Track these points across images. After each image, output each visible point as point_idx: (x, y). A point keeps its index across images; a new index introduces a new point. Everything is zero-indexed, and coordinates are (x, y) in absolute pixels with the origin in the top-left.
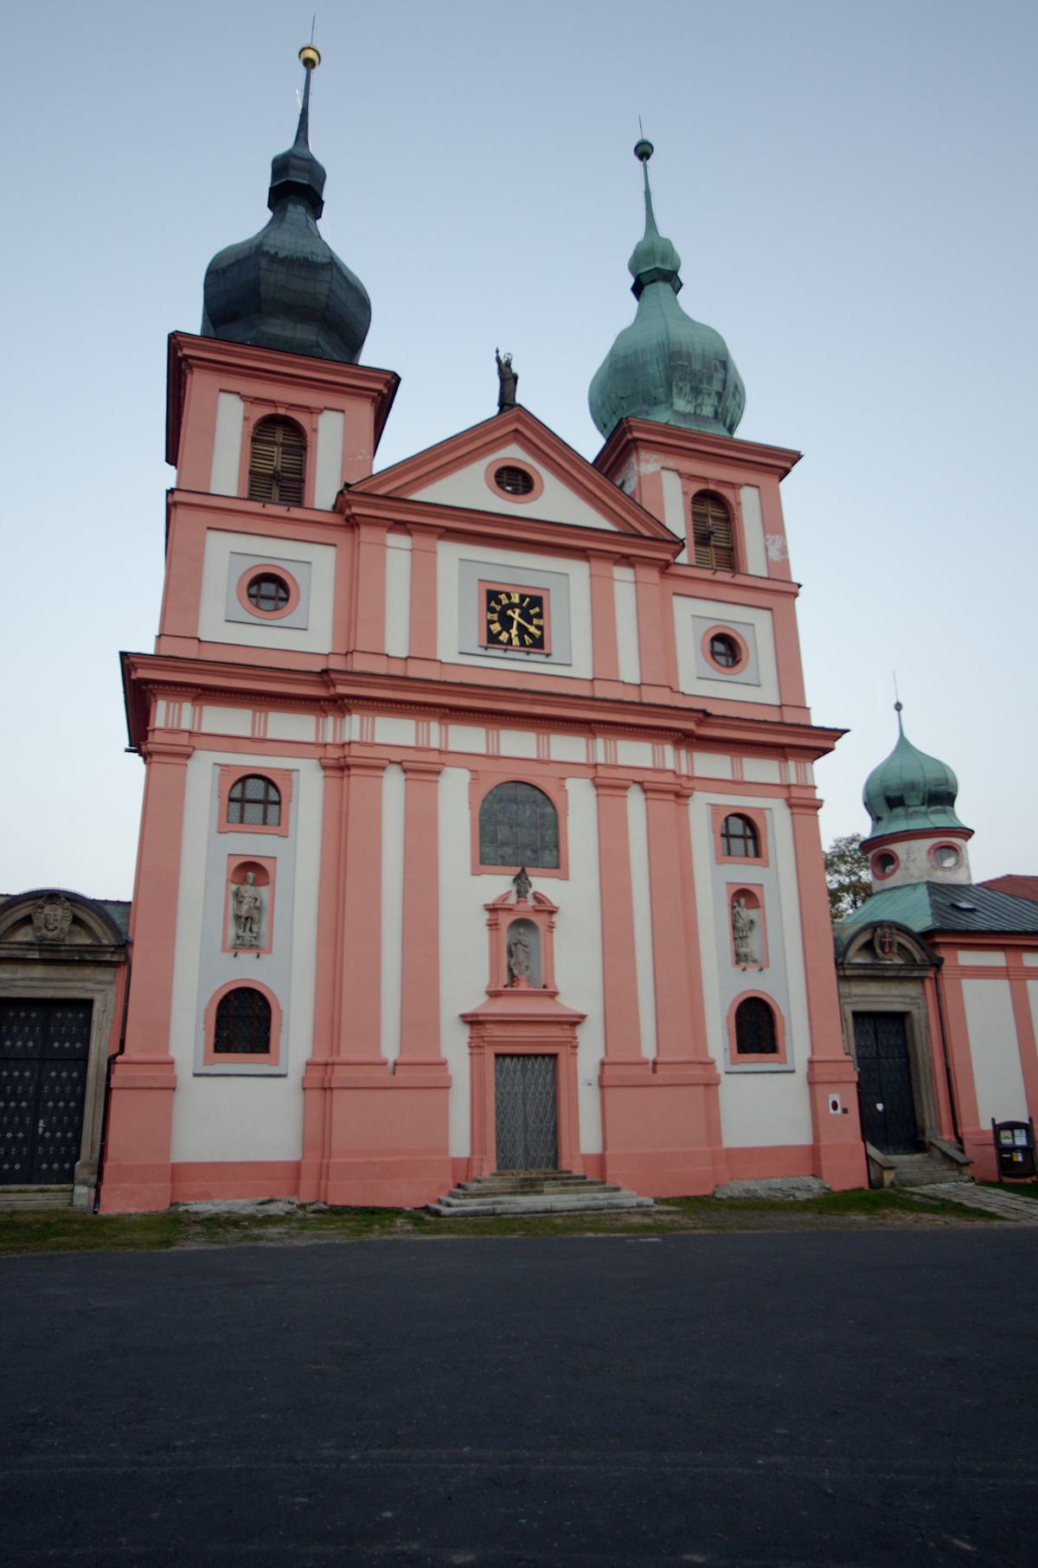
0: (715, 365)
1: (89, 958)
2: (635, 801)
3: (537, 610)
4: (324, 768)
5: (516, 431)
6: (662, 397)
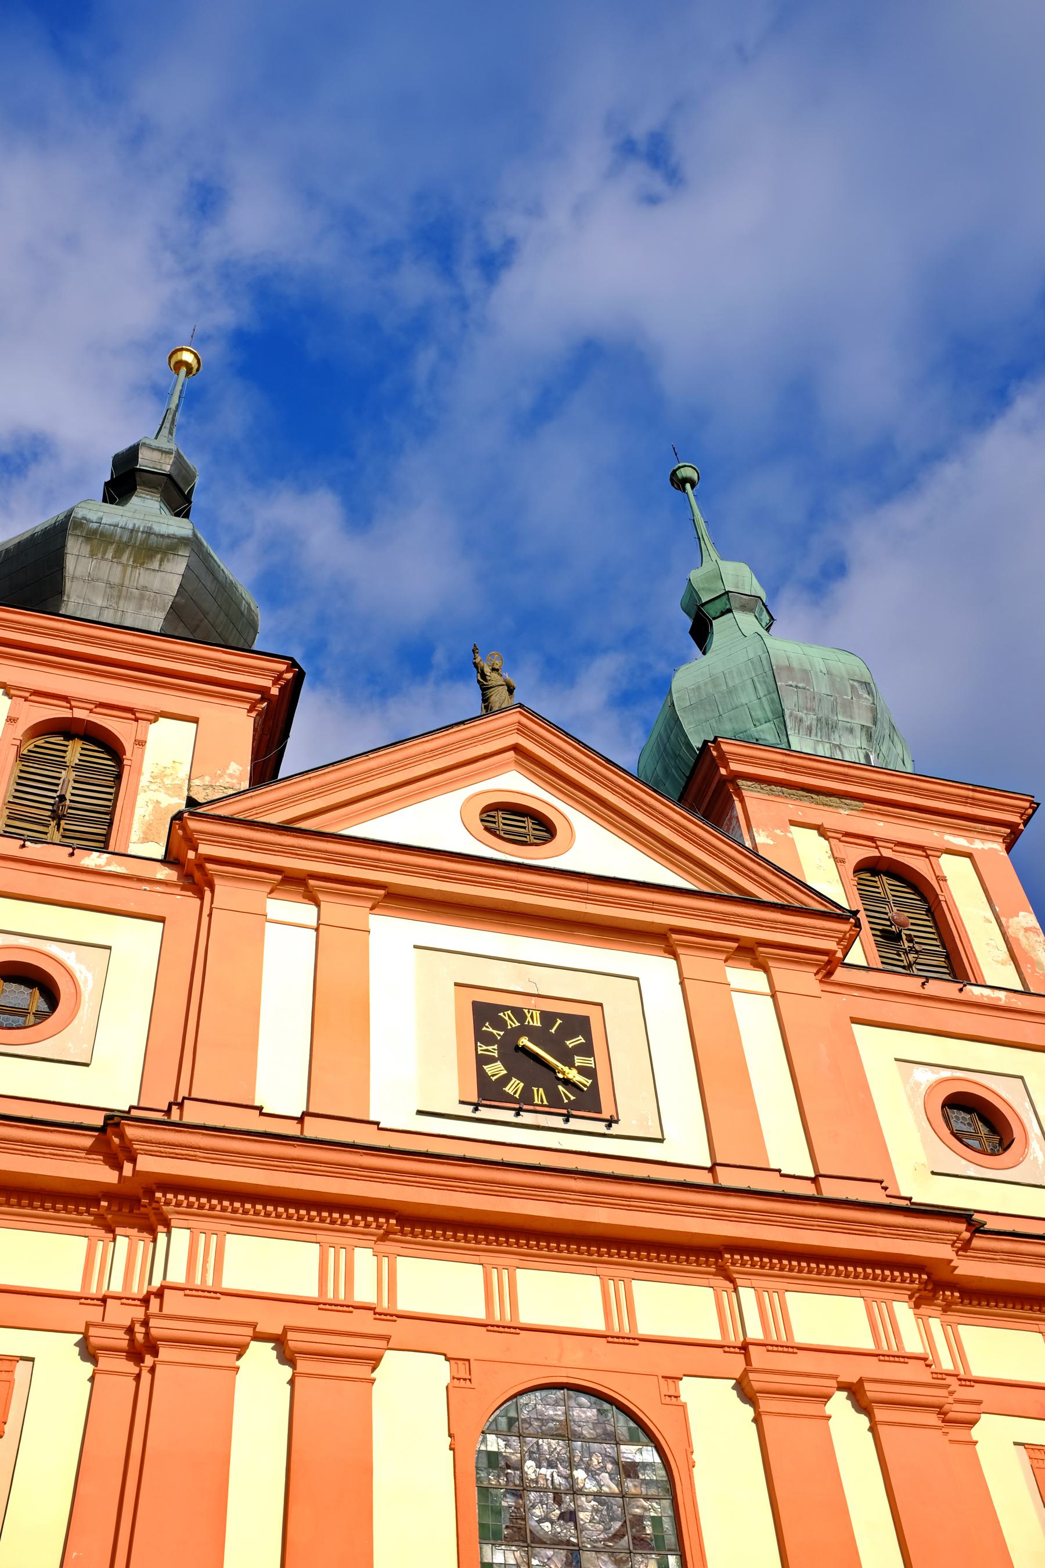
0: (852, 686)
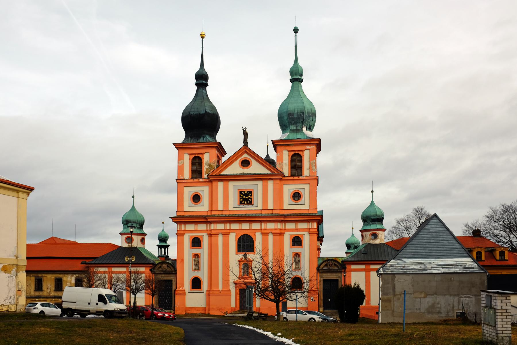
0: (301, 114)
1: (171, 273)
2: (271, 237)
3: (251, 194)
4: (208, 235)
5: (245, 151)
6: (288, 126)
